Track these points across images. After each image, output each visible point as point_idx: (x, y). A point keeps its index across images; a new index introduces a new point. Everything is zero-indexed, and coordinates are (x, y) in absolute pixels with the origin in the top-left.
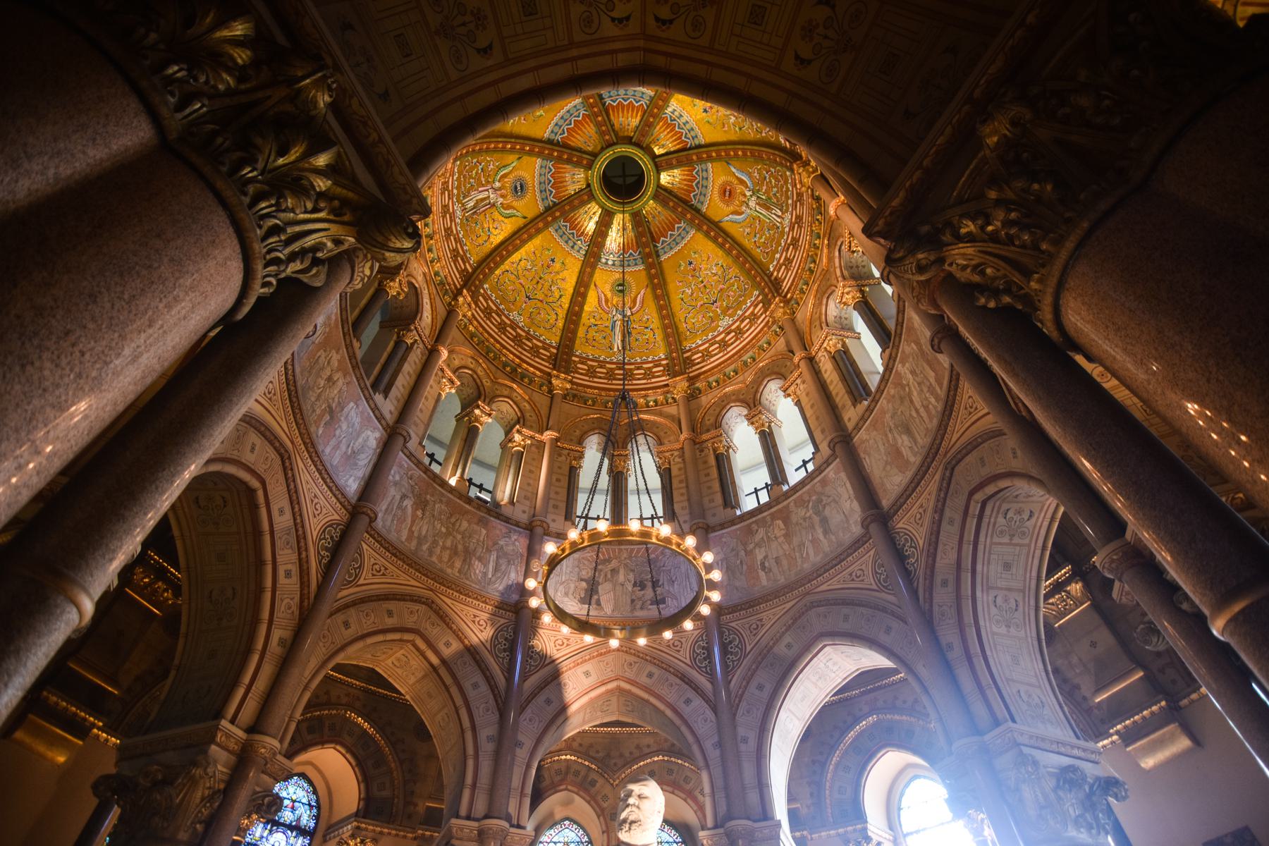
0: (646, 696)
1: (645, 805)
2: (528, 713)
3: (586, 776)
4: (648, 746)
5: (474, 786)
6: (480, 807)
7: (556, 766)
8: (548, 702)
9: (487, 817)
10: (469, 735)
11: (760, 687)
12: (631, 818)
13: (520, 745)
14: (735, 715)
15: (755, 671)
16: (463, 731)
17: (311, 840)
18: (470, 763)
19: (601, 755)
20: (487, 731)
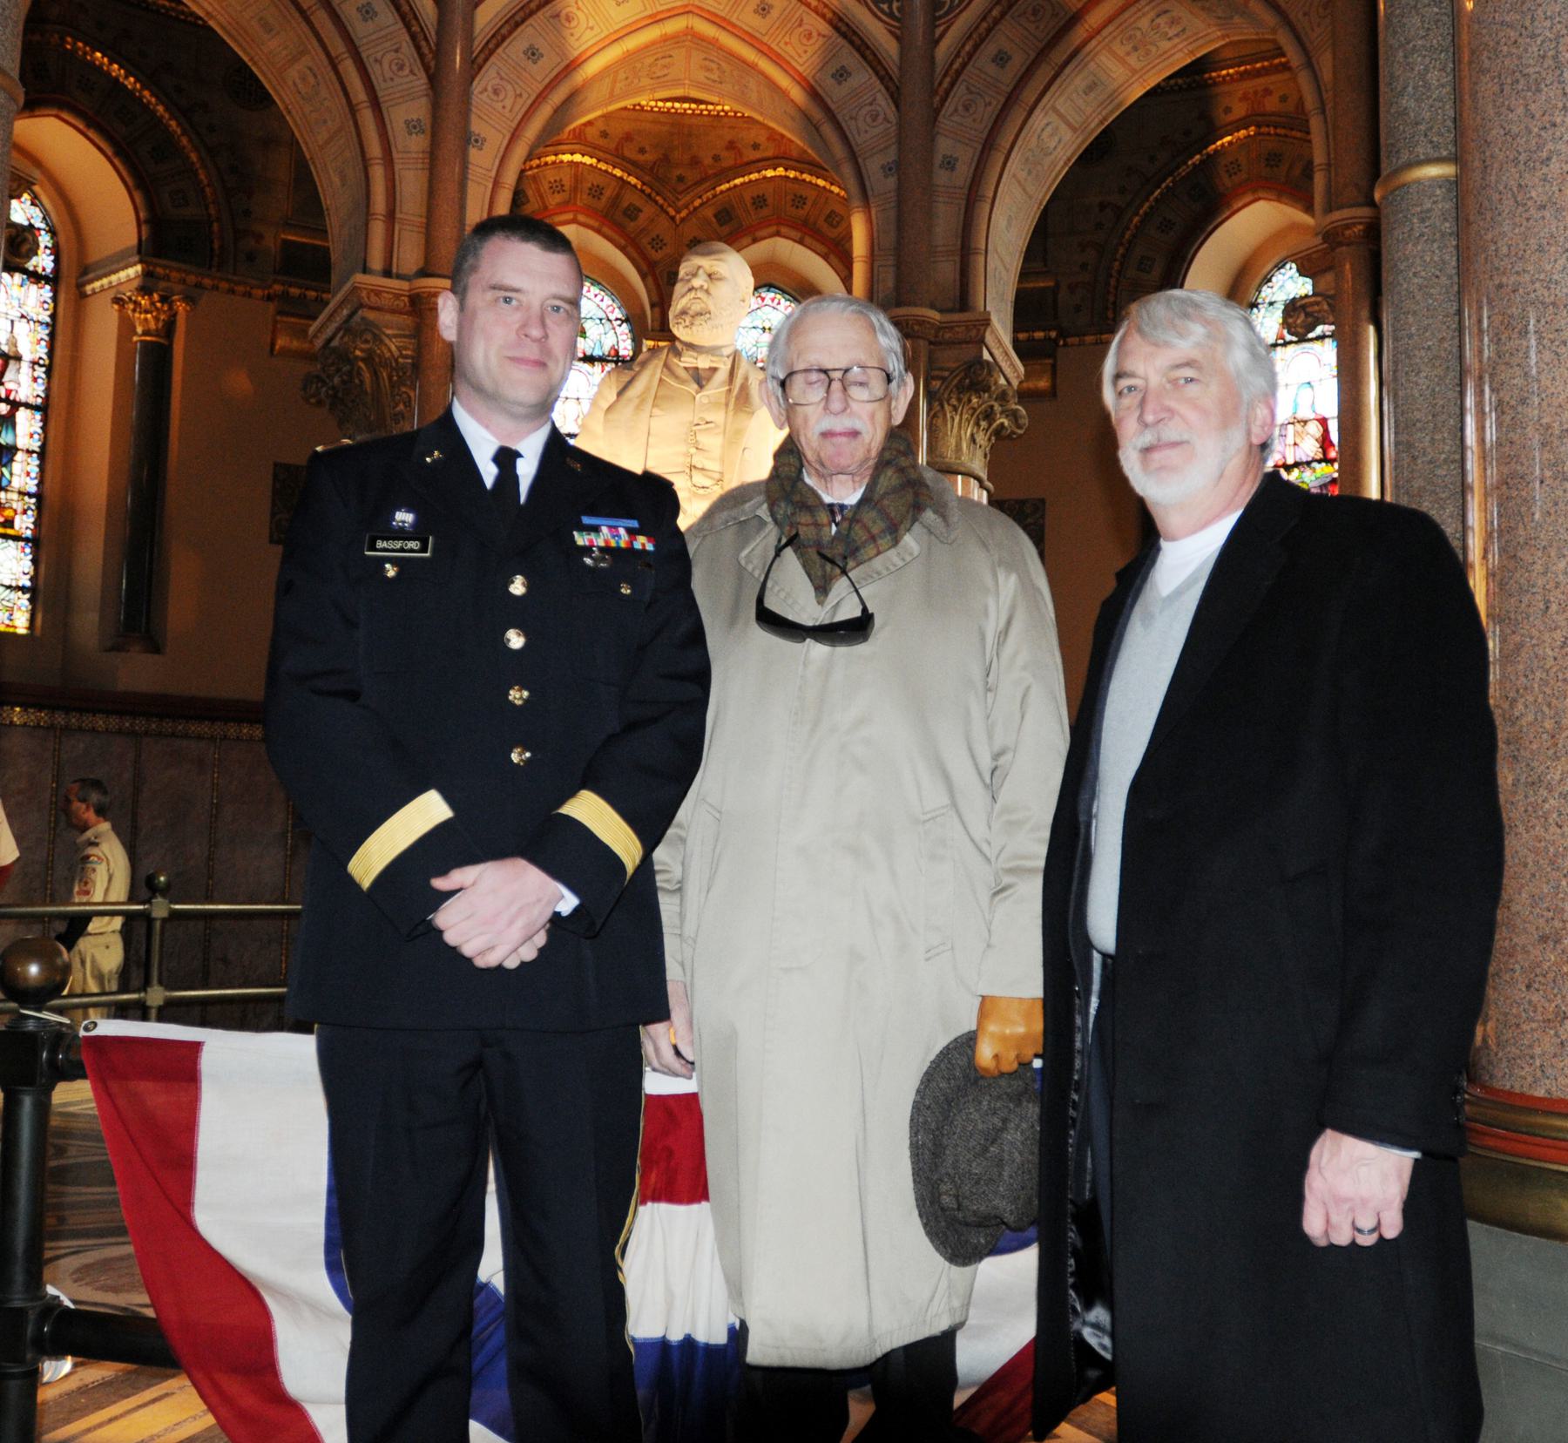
0: (749, 54)
1: (721, 290)
2: (488, 77)
3: (617, 198)
4: (756, 147)
5: (391, 216)
6: (409, 255)
7: (551, 176)
8: (533, 54)
9: (424, 273)
10: (367, 117)
11: (1001, 59)
12: (696, 307)
13: (480, 142)
14: (937, 111)
15: (996, 22)
16: (353, 109)
17: (55, 291)
18: (378, 173)
19: (649, 157)
20: (408, 109)
